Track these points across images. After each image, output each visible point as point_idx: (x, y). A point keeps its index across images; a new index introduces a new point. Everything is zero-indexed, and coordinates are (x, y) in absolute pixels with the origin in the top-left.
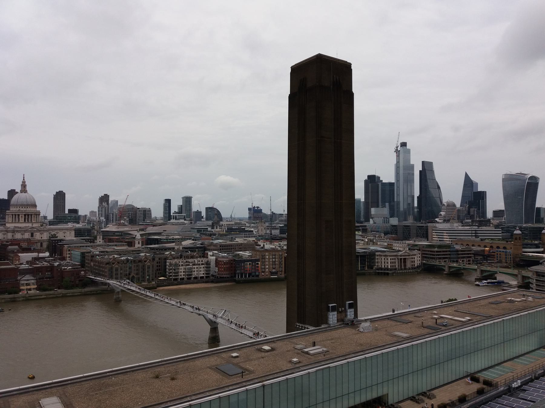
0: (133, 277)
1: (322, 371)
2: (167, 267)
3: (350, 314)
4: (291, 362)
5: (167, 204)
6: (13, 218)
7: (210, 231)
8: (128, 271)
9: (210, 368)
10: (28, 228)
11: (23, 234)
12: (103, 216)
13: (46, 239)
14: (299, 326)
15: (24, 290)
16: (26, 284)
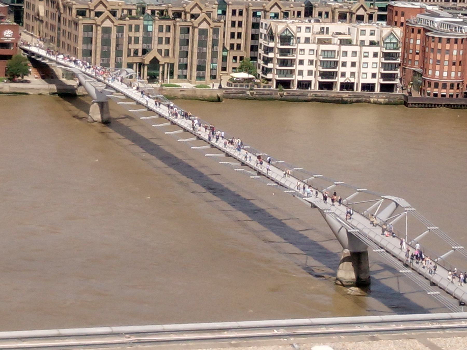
0: (155, 63)
8: (141, 42)
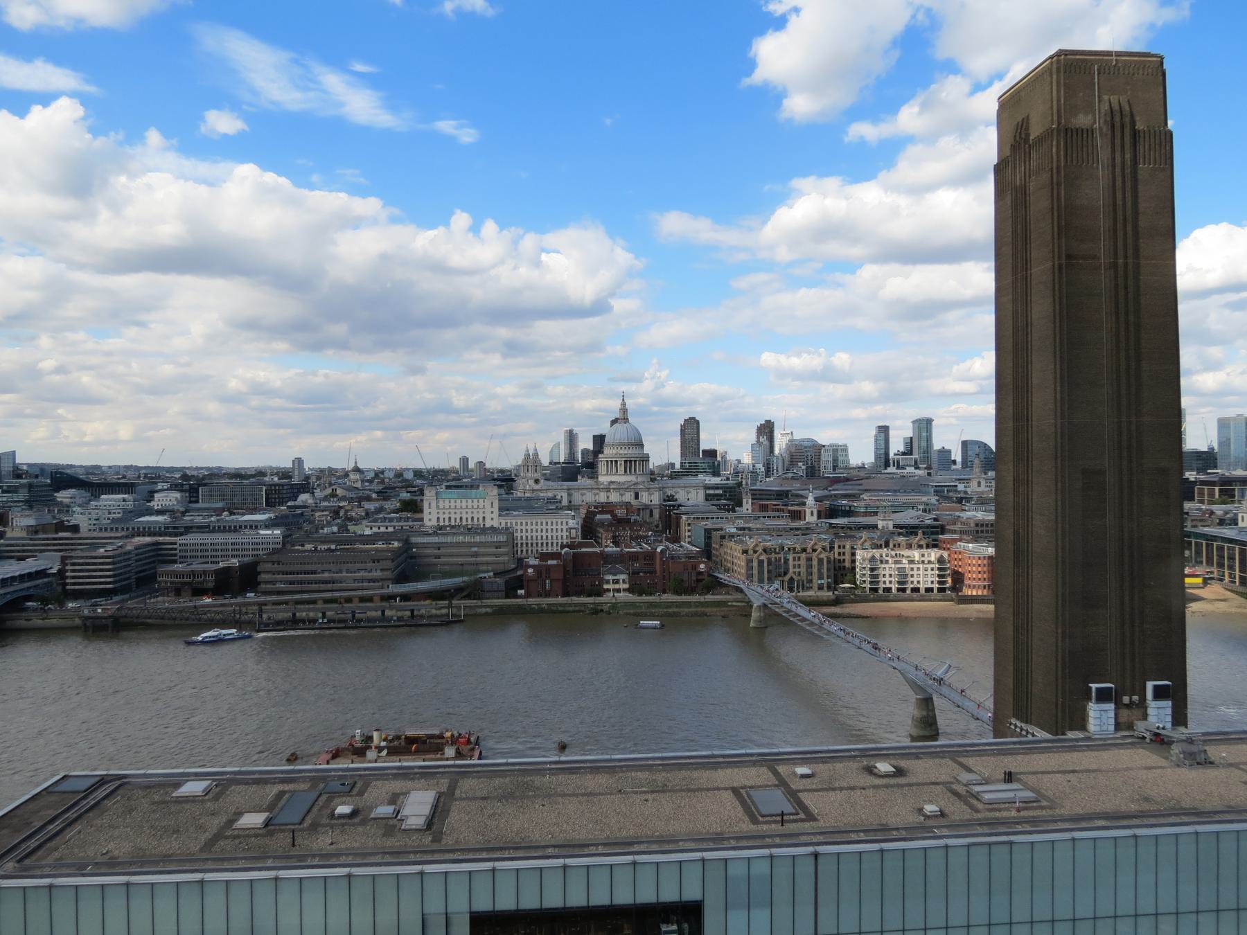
0: (792, 579)
1: (986, 849)
2: (857, 563)
3: (1159, 713)
4: (920, 810)
5: (883, 435)
6: (607, 466)
7: (960, 492)
9: (735, 791)
10: (631, 484)
11: (595, 495)
12: (761, 461)
13: (658, 503)
14: (1016, 726)
15: (608, 590)
16: (613, 580)
